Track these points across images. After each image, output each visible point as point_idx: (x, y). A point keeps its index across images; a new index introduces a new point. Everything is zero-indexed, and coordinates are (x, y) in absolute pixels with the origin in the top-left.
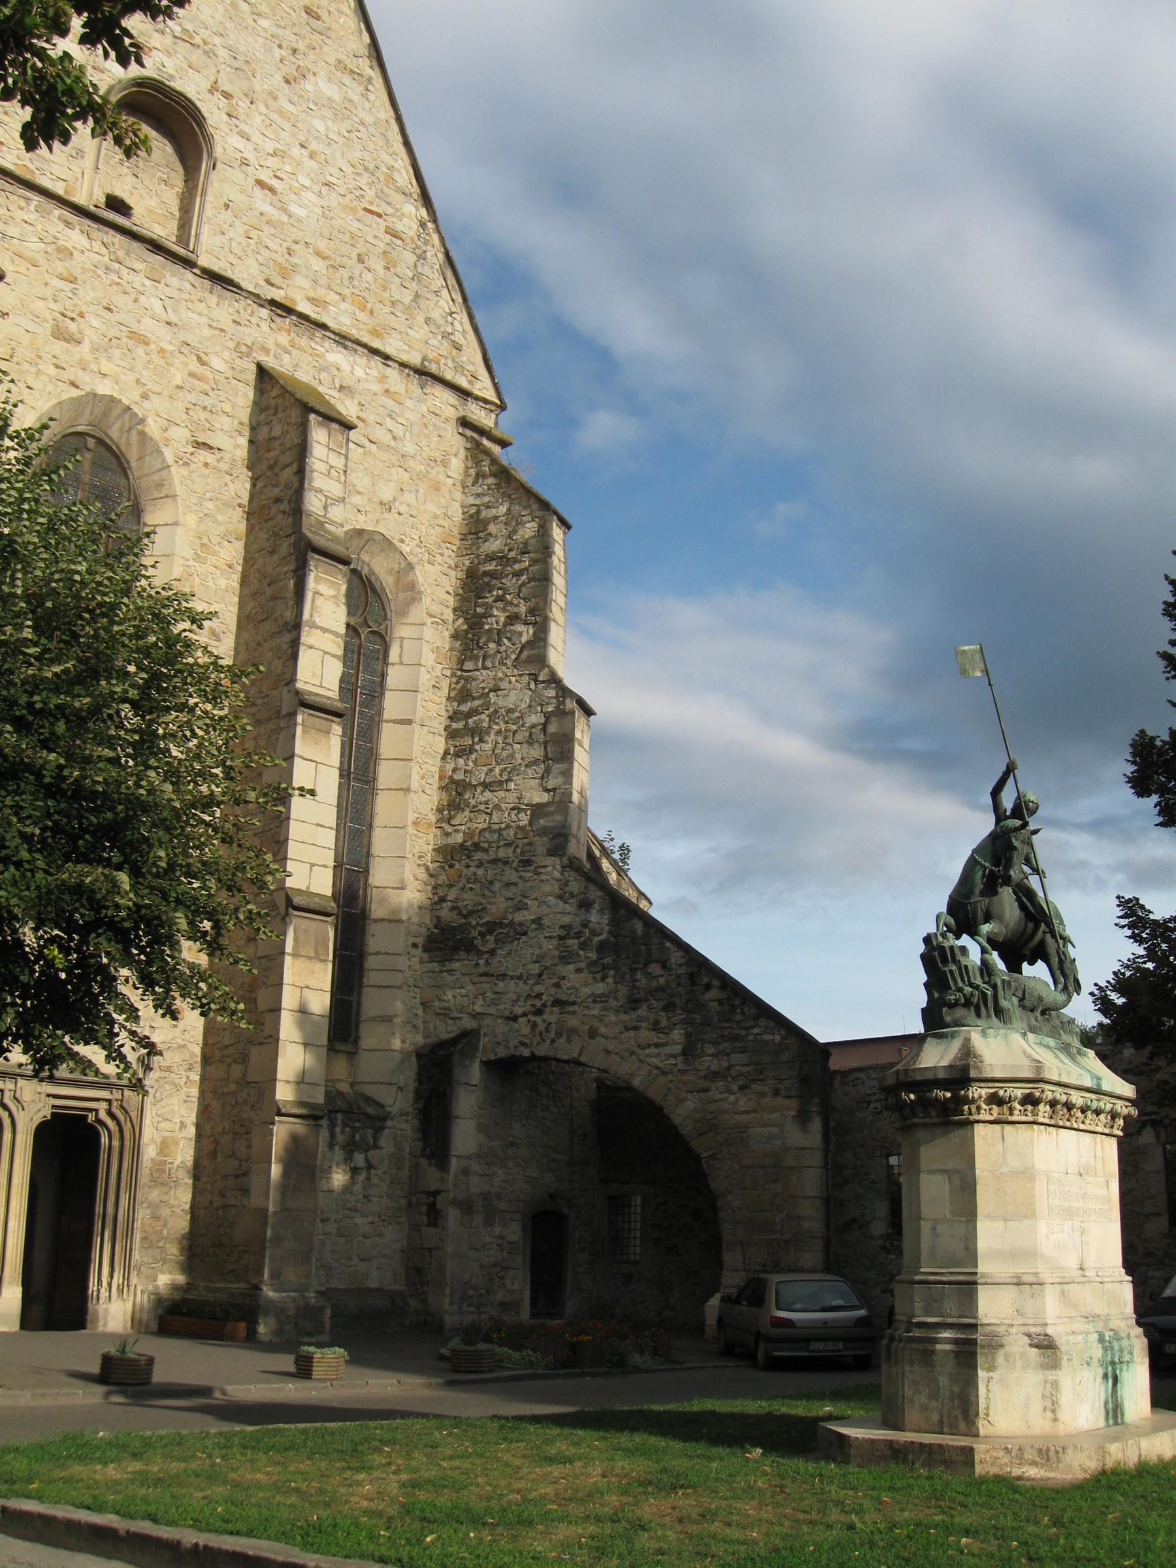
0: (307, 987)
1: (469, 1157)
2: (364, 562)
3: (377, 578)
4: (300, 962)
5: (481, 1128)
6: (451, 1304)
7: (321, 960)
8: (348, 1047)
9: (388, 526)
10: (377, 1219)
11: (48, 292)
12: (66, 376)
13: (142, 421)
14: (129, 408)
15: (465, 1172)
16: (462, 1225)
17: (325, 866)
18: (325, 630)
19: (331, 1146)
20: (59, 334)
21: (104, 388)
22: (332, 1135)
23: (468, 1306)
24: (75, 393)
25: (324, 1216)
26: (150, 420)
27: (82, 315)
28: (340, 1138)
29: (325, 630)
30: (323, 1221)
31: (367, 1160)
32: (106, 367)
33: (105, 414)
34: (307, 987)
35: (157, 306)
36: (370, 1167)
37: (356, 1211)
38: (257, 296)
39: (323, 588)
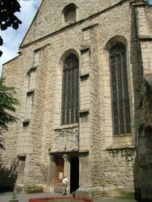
0: (84, 127)
1: (144, 155)
2: (118, 42)
3: (121, 42)
4: (83, 123)
5: (147, 147)
6: (143, 193)
7: (86, 121)
8: (130, 134)
9: (118, 33)
10: (136, 171)
11: (59, 43)
12: (62, 51)
13: (74, 49)
14: (71, 49)
15: (144, 158)
16: (144, 172)
17: (88, 103)
18: (85, 63)
19: (122, 156)
20: (61, 47)
21: (67, 49)
22: (122, 154)
23: (149, 193)
24: (64, 52)
25: (122, 172)
26: (75, 48)
27: (64, 42)
28: (124, 154)
29: (85, 63)
30: (122, 173)
31: (132, 158)
32: (67, 46)
33: (70, 52)
34: (84, 127)
35: (74, 32)
36: (133, 160)
37: (130, 170)
38: (87, 18)
39: (84, 56)
